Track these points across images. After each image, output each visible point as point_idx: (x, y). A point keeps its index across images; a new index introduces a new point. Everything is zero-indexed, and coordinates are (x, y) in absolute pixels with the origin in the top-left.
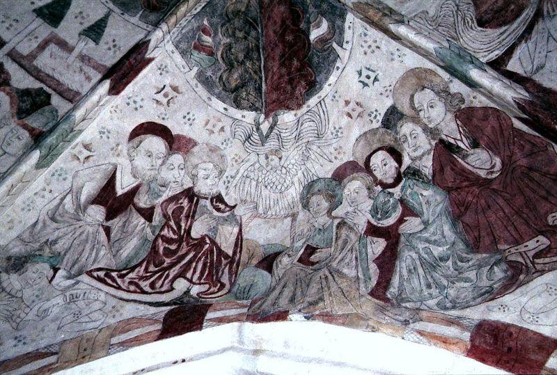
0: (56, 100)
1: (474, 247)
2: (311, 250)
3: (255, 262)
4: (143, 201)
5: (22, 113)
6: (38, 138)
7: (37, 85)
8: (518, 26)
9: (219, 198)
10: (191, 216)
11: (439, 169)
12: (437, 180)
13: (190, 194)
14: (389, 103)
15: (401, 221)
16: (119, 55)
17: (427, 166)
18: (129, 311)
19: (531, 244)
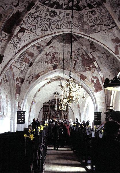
0: (41, 47)
1: (83, 66)
2: (68, 60)
3: (62, 60)
4: (50, 54)
5: (37, 49)
6: (39, 51)
7: (39, 45)
8: (94, 50)
9: (58, 53)
10: (55, 55)
11: (82, 56)
12: (81, 57)
13: (55, 52)
14: (79, 48)
15: (77, 60)
16: (49, 41)
17: (81, 55)
18: (50, 66)
19: (88, 67)
